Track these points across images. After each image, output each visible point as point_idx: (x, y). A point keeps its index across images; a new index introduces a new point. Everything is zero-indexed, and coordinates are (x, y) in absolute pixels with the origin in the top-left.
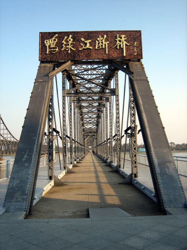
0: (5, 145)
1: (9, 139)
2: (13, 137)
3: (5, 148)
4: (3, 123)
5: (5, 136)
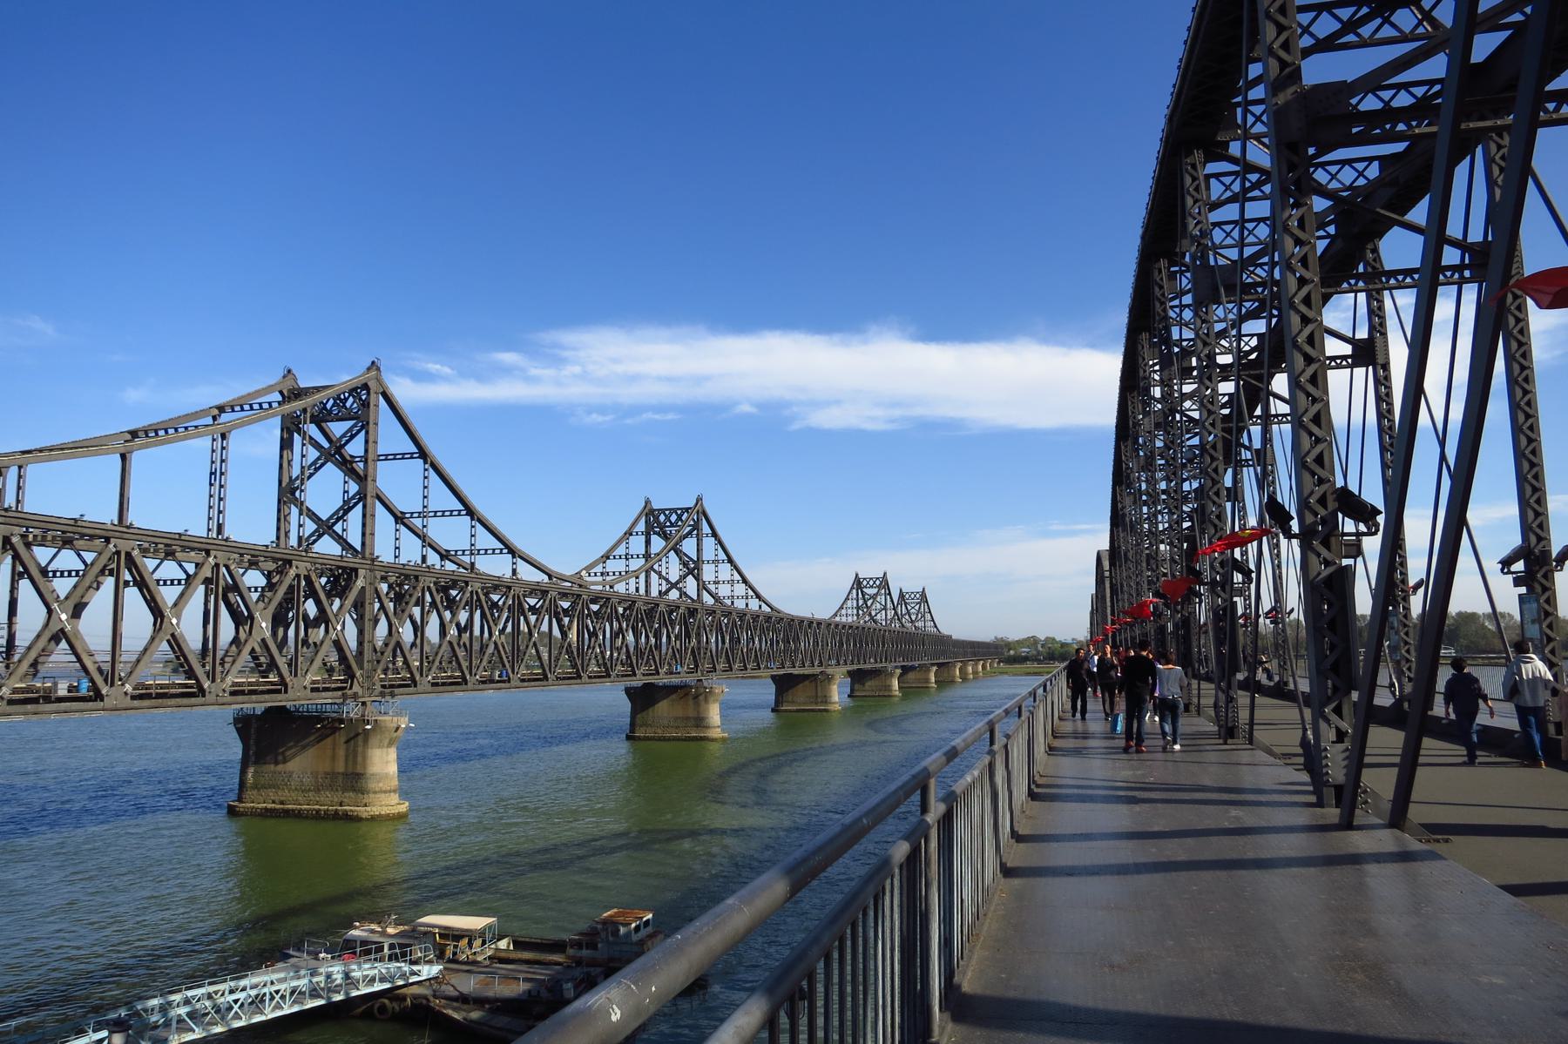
0: (721, 629)
1: (740, 604)
2: (758, 596)
3: (723, 642)
4: (714, 534)
5: (724, 591)
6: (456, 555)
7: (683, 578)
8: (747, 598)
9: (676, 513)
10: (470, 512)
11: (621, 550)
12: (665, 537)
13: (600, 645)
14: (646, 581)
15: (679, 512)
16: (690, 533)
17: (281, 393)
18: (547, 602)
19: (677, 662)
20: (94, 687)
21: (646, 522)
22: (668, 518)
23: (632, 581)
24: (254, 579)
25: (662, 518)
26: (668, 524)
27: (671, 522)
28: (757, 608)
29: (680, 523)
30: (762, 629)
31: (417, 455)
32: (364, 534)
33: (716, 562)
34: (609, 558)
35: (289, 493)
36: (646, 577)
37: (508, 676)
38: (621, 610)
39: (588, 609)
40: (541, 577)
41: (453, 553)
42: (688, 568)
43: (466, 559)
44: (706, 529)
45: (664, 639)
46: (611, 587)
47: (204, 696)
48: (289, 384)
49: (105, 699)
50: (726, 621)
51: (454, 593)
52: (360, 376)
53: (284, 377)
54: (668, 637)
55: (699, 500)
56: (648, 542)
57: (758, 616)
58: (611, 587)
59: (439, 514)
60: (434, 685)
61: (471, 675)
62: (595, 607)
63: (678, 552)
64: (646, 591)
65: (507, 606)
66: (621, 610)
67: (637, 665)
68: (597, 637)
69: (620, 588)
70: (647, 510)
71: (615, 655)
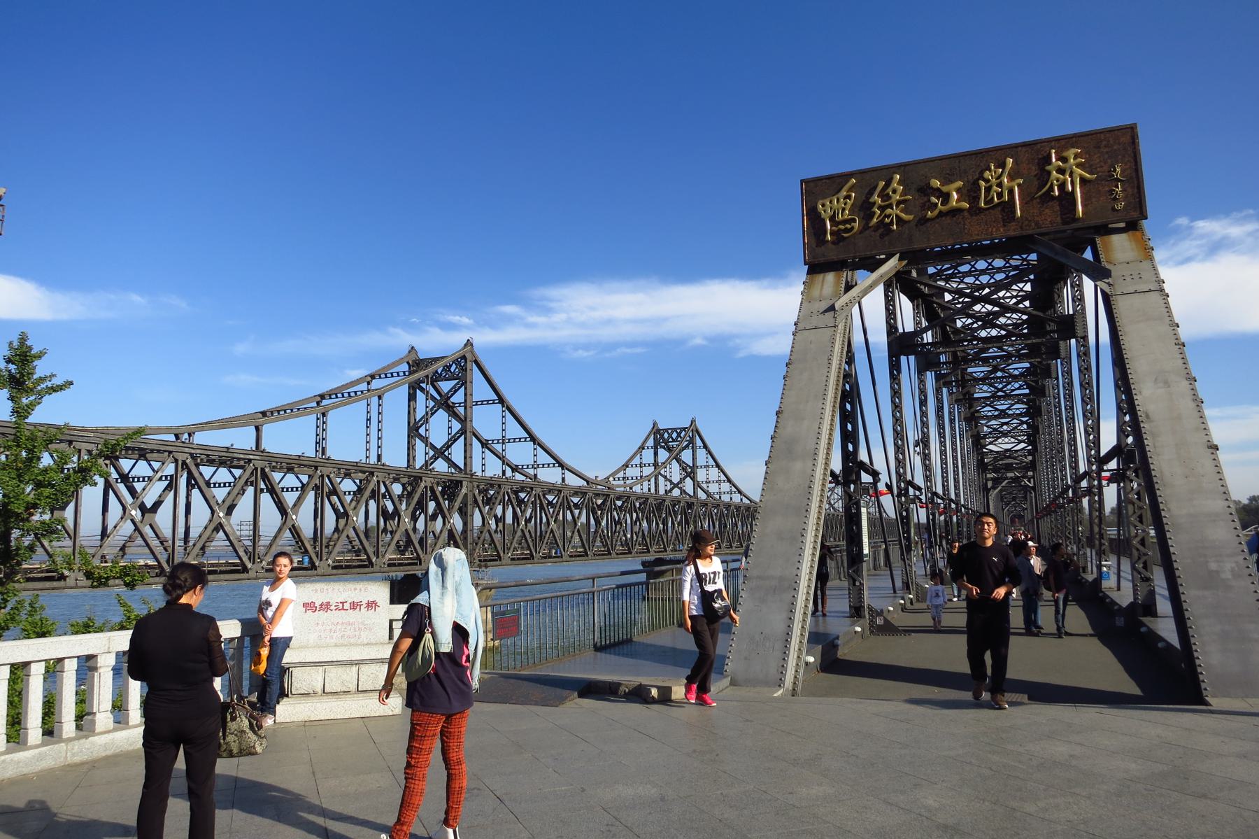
0: (712, 517)
1: (726, 498)
2: (740, 492)
4: (705, 447)
5: (713, 488)
6: (522, 468)
7: (682, 480)
8: (731, 494)
9: (677, 432)
10: (533, 439)
11: (636, 461)
12: (669, 450)
13: (623, 531)
14: (656, 483)
15: (678, 431)
16: (687, 446)
17: (408, 363)
18: (586, 501)
19: (679, 542)
20: (311, 561)
21: (654, 439)
22: (670, 435)
23: (646, 484)
24: (397, 489)
25: (666, 435)
26: (670, 440)
27: (672, 438)
28: (740, 501)
29: (679, 439)
30: (743, 515)
31: (497, 401)
32: (465, 458)
33: (707, 467)
34: (628, 467)
35: (414, 430)
36: (656, 479)
37: (561, 553)
38: (637, 505)
39: (615, 505)
40: (582, 483)
41: (520, 467)
42: (686, 472)
43: (531, 471)
44: (699, 442)
45: (670, 525)
46: (631, 488)
47: (372, 567)
48: (413, 357)
49: (318, 569)
50: (715, 511)
51: (522, 495)
52: (460, 351)
53: (409, 352)
54: (673, 523)
55: (693, 421)
56: (656, 454)
57: (740, 507)
58: (631, 488)
59: (512, 440)
60: (513, 559)
61: (536, 553)
62: (619, 503)
63: (678, 461)
64: (656, 490)
65: (530, 502)
66: (637, 505)
67: (651, 545)
68: (621, 524)
69: (637, 489)
70: (654, 430)
71: (635, 537)
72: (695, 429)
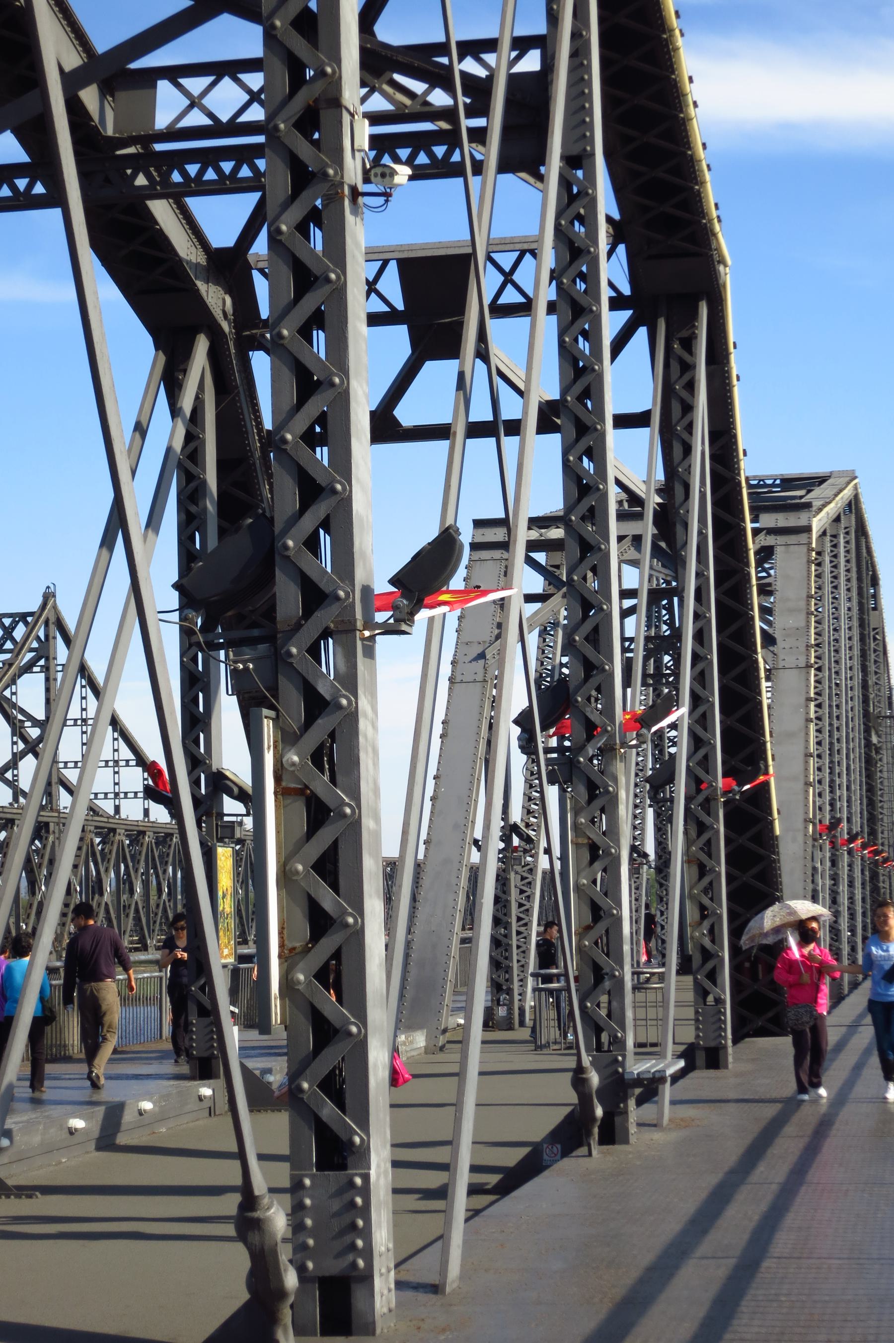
1: (133, 810)
55: (48, 596)
72: (52, 619)
